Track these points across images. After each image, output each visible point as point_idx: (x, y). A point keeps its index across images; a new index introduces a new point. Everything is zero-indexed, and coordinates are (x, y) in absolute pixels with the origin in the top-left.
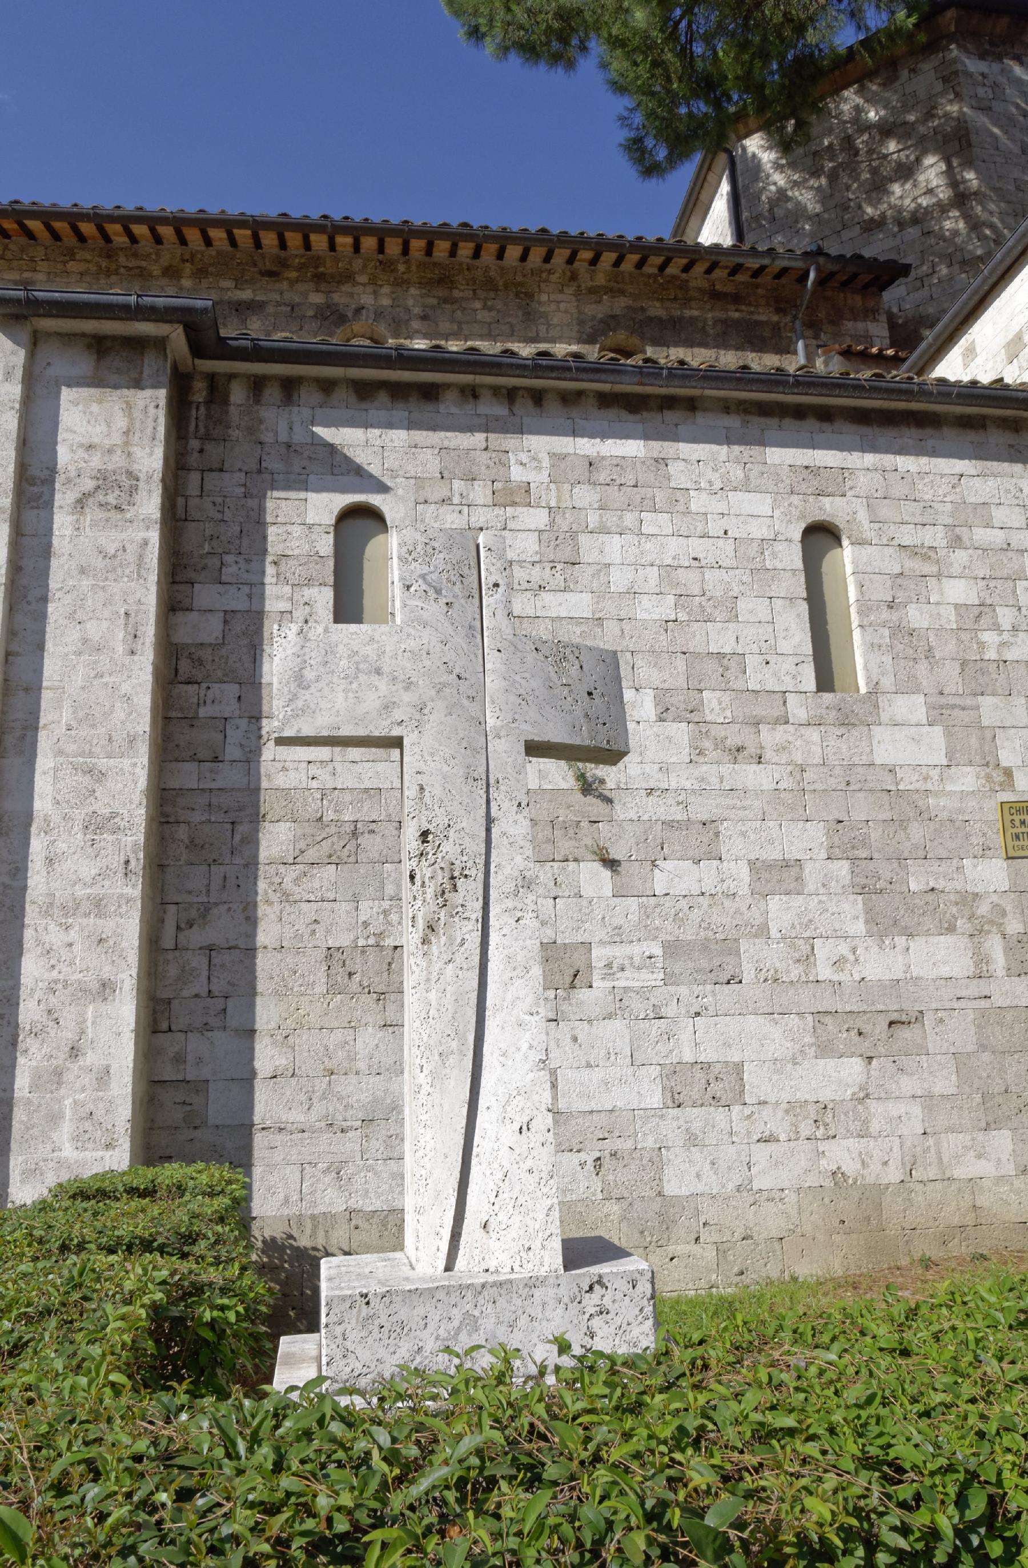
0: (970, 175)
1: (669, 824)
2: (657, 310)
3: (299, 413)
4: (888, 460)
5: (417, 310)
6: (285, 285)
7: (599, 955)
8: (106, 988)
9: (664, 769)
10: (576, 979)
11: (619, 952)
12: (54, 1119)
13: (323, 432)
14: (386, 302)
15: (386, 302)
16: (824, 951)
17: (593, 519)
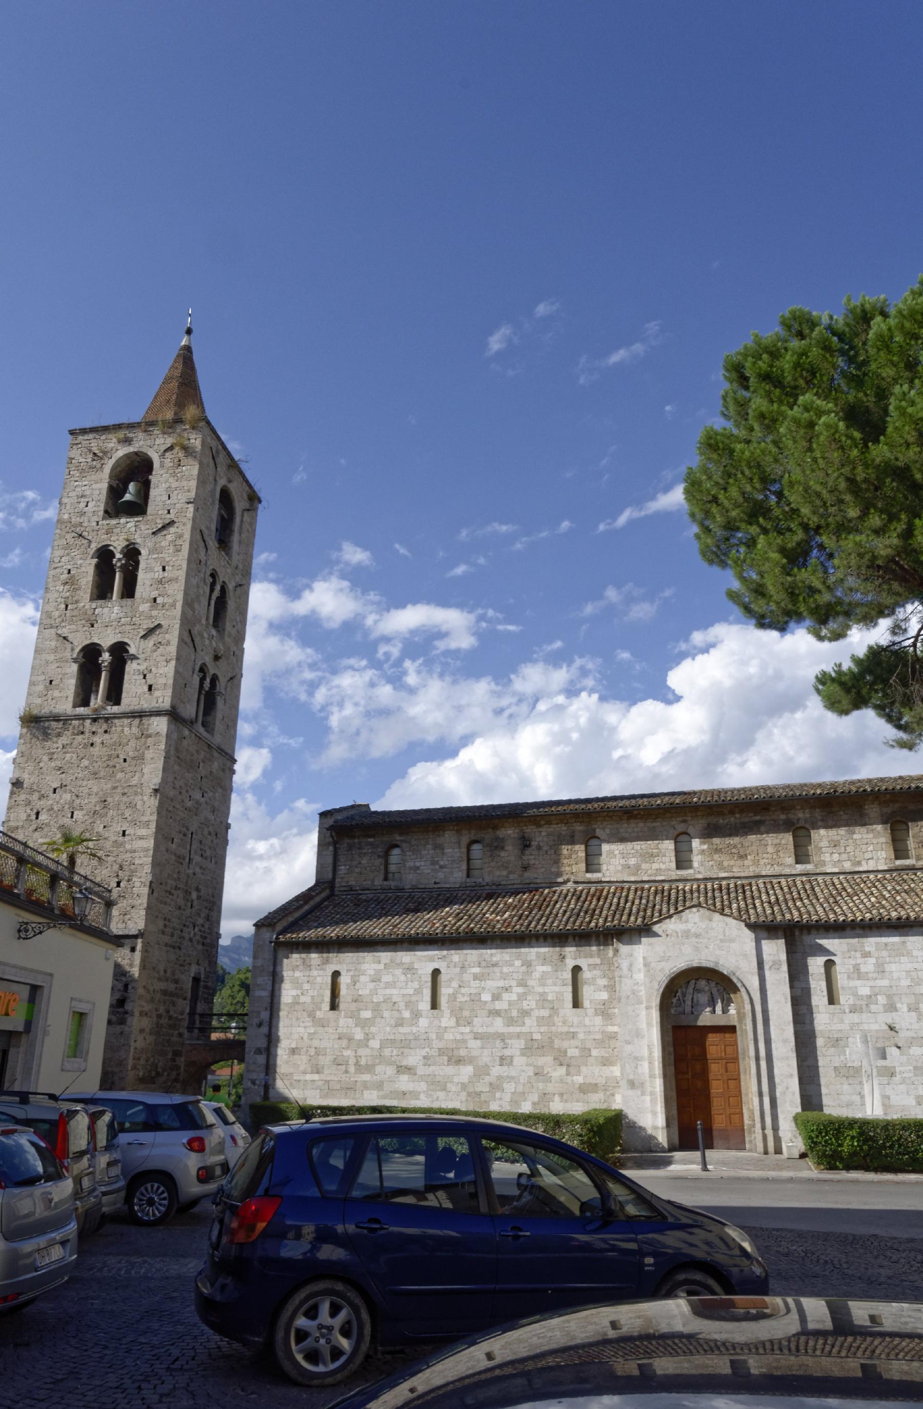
1: (913, 1038)
2: (912, 807)
5: (819, 818)
7: (898, 1069)
8: (791, 1075)
9: (911, 1024)
10: (892, 1075)
11: (902, 1069)
13: (817, 941)
15: (808, 815)
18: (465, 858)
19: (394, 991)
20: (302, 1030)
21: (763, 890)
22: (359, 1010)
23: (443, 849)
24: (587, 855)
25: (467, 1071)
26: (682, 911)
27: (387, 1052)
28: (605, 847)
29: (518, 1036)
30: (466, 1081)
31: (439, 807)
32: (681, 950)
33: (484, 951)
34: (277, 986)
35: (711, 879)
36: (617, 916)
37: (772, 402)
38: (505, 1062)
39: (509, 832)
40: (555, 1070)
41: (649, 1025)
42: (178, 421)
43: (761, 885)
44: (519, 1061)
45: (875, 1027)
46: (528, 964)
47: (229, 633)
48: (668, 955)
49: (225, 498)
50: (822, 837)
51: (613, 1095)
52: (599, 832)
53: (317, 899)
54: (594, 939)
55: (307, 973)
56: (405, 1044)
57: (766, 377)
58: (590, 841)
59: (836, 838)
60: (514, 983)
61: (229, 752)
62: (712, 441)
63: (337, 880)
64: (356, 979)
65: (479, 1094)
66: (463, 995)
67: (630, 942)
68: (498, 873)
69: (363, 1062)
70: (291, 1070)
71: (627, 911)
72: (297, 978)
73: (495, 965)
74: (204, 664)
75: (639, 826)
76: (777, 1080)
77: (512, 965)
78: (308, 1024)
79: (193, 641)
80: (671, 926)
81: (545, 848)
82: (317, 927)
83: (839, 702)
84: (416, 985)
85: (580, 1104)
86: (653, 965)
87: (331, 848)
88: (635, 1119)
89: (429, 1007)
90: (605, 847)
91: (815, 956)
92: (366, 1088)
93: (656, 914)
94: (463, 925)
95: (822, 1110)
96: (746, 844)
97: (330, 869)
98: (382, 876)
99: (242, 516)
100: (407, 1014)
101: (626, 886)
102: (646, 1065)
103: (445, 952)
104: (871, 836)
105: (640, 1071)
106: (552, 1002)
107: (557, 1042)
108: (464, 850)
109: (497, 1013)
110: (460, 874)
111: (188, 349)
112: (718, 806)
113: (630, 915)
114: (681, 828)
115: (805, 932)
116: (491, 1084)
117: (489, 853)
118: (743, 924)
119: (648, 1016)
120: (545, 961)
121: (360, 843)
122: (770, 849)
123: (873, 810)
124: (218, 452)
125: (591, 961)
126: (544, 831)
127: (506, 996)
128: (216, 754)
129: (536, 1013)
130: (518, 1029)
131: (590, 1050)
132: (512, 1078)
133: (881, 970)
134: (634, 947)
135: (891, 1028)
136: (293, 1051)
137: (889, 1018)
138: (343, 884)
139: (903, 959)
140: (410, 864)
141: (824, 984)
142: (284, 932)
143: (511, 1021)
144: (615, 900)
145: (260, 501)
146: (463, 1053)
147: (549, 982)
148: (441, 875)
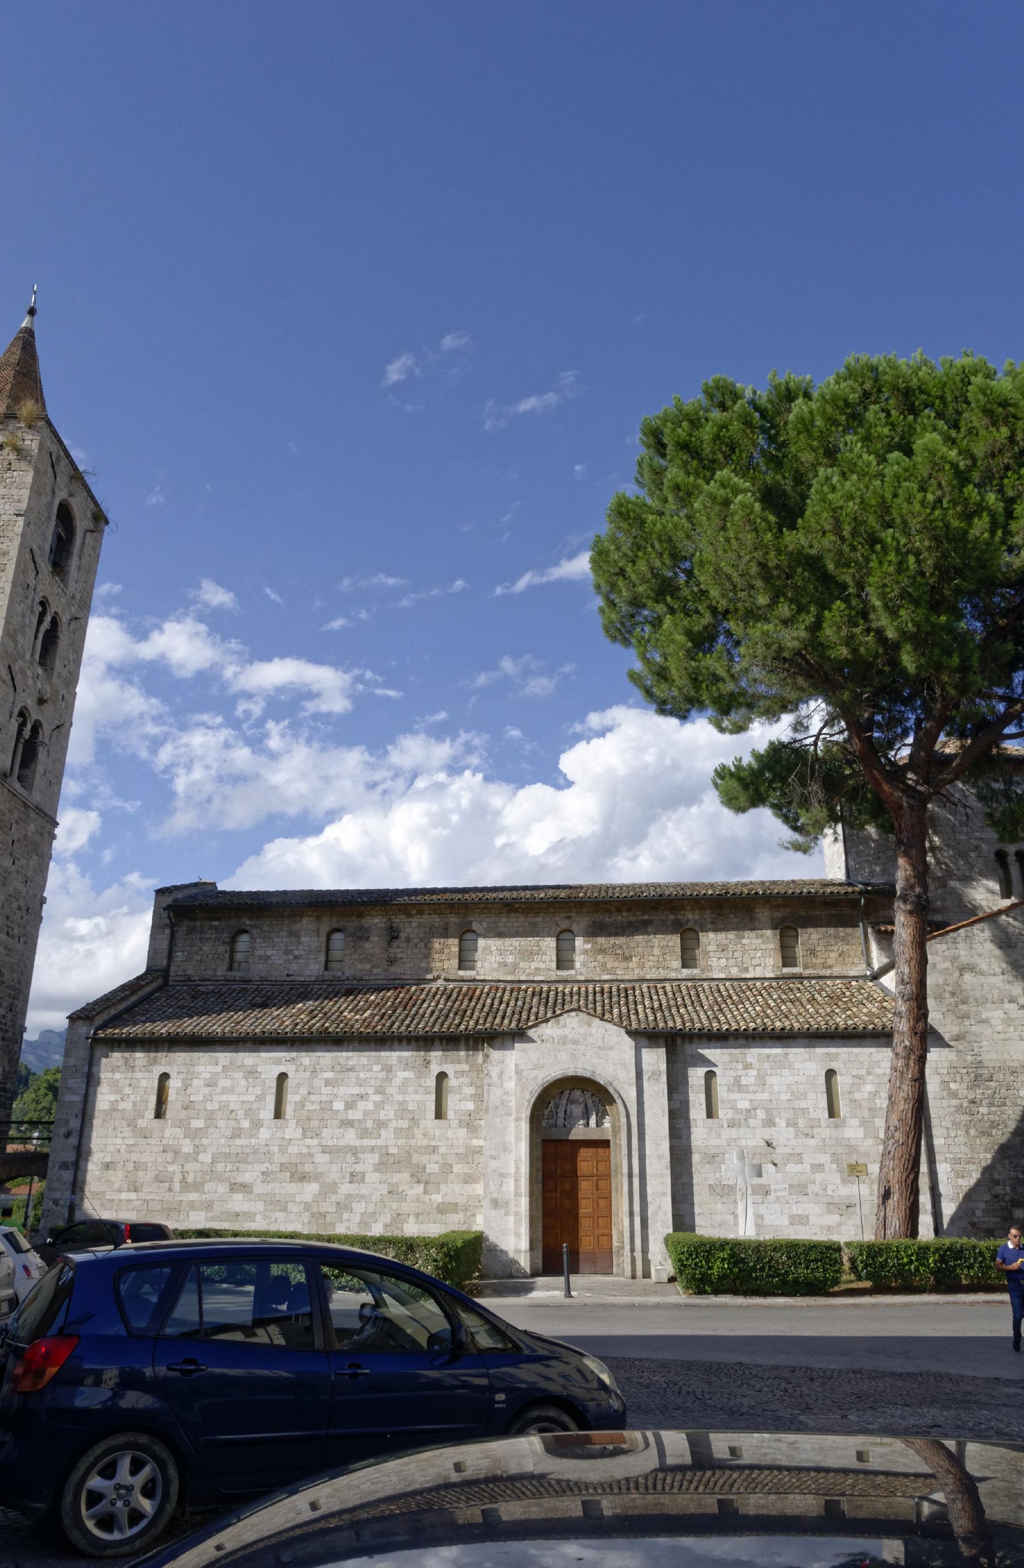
0: (936, 839)
1: (790, 1154)
2: (803, 913)
3: (694, 1046)
4: (850, 1049)
6: (660, 912)
7: (772, 1188)
8: (664, 1194)
9: (788, 1140)
10: (767, 1193)
12: (657, 1222)
14: (697, 917)
15: (697, 917)
16: (830, 1188)
17: (769, 1072)
18: (324, 948)
19: (233, 1098)
20: (119, 1141)
21: (646, 995)
22: (189, 1119)
23: (299, 938)
24: (461, 950)
25: (311, 1189)
26: (560, 1015)
27: (220, 1167)
28: (482, 942)
29: (373, 1149)
30: (310, 1200)
31: (297, 889)
32: (556, 1057)
33: (339, 1054)
34: (91, 1089)
35: (593, 981)
36: (490, 1019)
37: (688, 474)
38: (355, 1179)
39: (376, 921)
40: (412, 1188)
41: (518, 1138)
42: (11, 416)
43: (645, 990)
44: (372, 1177)
45: (752, 1143)
46: (388, 1069)
47: (59, 673)
48: (542, 1062)
49: (65, 514)
50: (710, 940)
51: (474, 1215)
52: (475, 926)
53: (148, 990)
54: (463, 1042)
55: (130, 1075)
56: (241, 1159)
57: (684, 446)
58: (466, 935)
59: (724, 942)
60: (371, 1090)
61: (50, 813)
62: (623, 509)
63: (172, 968)
64: (188, 1082)
65: (324, 1215)
66: (313, 1103)
67: (503, 1048)
68: (360, 966)
69: (190, 1179)
70: (104, 1188)
71: (500, 1014)
72: (118, 1081)
73: (351, 1069)
74: (25, 708)
75: (520, 920)
76: (649, 1199)
77: (371, 1070)
78: (127, 1134)
79: (13, 679)
80: (547, 1030)
81: (415, 941)
82: (145, 1022)
83: (737, 798)
84: (258, 1090)
85: (437, 1225)
86: (525, 1073)
87: (168, 931)
88: (497, 1242)
89: (272, 1116)
90: (482, 942)
91: (696, 1066)
92: (193, 1208)
93: (532, 1018)
94: (317, 1024)
95: (694, 1231)
96: (632, 945)
97: (165, 955)
98: (225, 965)
99: (84, 537)
100: (246, 1124)
101: (502, 985)
102: (511, 1182)
103: (294, 1054)
104: (760, 941)
105: (504, 1188)
106: (412, 1112)
107: (415, 1156)
108: (324, 939)
109: (348, 1124)
110: (317, 966)
111: (29, 332)
112: (606, 903)
113: (503, 1018)
114: (564, 924)
115: (687, 1040)
116: (338, 1203)
117: (352, 944)
118: (623, 1031)
119: (517, 1127)
120: (407, 1067)
121: (202, 927)
122: (656, 952)
123: (763, 914)
124: (58, 459)
125: (459, 1067)
126: (415, 921)
127: (361, 1105)
128: (33, 815)
129: (394, 1124)
130: (372, 1142)
131: (451, 1166)
132: (363, 1196)
133: (761, 1081)
134: (506, 1052)
135: (769, 1144)
136: (107, 1166)
137: (768, 1133)
138: (179, 973)
139: (785, 1072)
140: (260, 952)
141: (703, 1097)
142: (104, 1026)
143: (365, 1133)
144: (489, 1001)
145: (107, 522)
146: (308, 1168)
147: (410, 1089)
148: (295, 967)
